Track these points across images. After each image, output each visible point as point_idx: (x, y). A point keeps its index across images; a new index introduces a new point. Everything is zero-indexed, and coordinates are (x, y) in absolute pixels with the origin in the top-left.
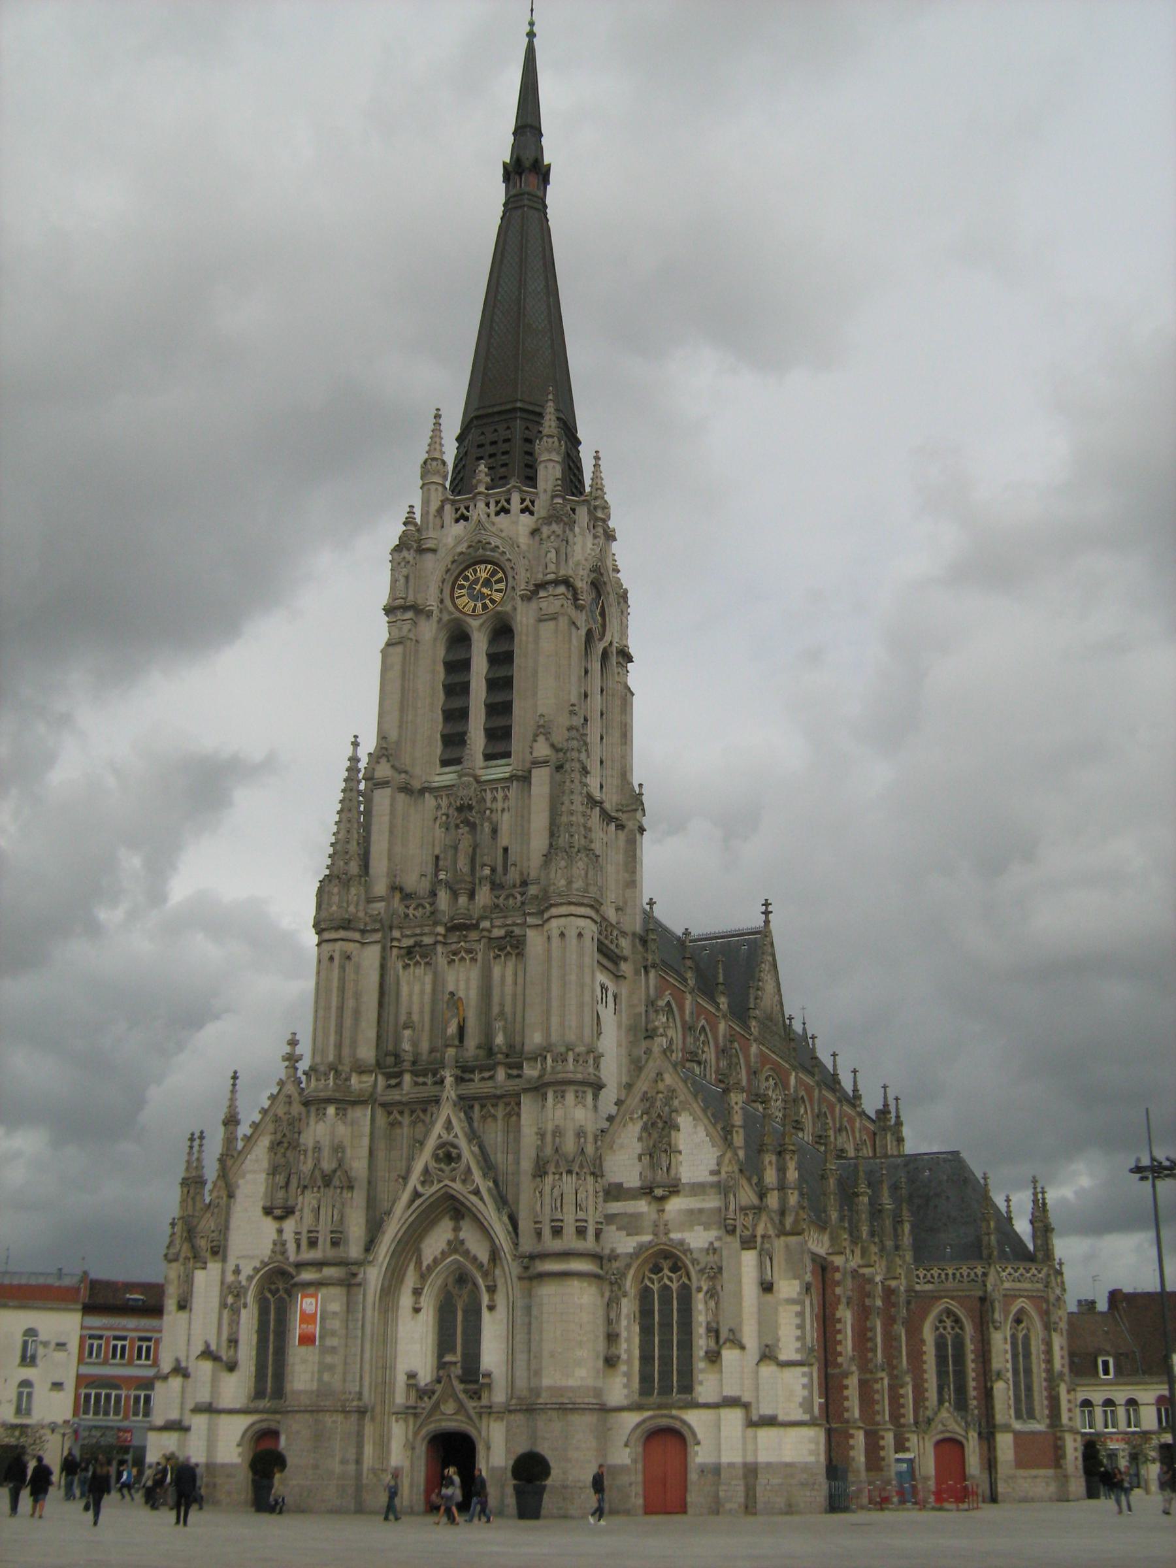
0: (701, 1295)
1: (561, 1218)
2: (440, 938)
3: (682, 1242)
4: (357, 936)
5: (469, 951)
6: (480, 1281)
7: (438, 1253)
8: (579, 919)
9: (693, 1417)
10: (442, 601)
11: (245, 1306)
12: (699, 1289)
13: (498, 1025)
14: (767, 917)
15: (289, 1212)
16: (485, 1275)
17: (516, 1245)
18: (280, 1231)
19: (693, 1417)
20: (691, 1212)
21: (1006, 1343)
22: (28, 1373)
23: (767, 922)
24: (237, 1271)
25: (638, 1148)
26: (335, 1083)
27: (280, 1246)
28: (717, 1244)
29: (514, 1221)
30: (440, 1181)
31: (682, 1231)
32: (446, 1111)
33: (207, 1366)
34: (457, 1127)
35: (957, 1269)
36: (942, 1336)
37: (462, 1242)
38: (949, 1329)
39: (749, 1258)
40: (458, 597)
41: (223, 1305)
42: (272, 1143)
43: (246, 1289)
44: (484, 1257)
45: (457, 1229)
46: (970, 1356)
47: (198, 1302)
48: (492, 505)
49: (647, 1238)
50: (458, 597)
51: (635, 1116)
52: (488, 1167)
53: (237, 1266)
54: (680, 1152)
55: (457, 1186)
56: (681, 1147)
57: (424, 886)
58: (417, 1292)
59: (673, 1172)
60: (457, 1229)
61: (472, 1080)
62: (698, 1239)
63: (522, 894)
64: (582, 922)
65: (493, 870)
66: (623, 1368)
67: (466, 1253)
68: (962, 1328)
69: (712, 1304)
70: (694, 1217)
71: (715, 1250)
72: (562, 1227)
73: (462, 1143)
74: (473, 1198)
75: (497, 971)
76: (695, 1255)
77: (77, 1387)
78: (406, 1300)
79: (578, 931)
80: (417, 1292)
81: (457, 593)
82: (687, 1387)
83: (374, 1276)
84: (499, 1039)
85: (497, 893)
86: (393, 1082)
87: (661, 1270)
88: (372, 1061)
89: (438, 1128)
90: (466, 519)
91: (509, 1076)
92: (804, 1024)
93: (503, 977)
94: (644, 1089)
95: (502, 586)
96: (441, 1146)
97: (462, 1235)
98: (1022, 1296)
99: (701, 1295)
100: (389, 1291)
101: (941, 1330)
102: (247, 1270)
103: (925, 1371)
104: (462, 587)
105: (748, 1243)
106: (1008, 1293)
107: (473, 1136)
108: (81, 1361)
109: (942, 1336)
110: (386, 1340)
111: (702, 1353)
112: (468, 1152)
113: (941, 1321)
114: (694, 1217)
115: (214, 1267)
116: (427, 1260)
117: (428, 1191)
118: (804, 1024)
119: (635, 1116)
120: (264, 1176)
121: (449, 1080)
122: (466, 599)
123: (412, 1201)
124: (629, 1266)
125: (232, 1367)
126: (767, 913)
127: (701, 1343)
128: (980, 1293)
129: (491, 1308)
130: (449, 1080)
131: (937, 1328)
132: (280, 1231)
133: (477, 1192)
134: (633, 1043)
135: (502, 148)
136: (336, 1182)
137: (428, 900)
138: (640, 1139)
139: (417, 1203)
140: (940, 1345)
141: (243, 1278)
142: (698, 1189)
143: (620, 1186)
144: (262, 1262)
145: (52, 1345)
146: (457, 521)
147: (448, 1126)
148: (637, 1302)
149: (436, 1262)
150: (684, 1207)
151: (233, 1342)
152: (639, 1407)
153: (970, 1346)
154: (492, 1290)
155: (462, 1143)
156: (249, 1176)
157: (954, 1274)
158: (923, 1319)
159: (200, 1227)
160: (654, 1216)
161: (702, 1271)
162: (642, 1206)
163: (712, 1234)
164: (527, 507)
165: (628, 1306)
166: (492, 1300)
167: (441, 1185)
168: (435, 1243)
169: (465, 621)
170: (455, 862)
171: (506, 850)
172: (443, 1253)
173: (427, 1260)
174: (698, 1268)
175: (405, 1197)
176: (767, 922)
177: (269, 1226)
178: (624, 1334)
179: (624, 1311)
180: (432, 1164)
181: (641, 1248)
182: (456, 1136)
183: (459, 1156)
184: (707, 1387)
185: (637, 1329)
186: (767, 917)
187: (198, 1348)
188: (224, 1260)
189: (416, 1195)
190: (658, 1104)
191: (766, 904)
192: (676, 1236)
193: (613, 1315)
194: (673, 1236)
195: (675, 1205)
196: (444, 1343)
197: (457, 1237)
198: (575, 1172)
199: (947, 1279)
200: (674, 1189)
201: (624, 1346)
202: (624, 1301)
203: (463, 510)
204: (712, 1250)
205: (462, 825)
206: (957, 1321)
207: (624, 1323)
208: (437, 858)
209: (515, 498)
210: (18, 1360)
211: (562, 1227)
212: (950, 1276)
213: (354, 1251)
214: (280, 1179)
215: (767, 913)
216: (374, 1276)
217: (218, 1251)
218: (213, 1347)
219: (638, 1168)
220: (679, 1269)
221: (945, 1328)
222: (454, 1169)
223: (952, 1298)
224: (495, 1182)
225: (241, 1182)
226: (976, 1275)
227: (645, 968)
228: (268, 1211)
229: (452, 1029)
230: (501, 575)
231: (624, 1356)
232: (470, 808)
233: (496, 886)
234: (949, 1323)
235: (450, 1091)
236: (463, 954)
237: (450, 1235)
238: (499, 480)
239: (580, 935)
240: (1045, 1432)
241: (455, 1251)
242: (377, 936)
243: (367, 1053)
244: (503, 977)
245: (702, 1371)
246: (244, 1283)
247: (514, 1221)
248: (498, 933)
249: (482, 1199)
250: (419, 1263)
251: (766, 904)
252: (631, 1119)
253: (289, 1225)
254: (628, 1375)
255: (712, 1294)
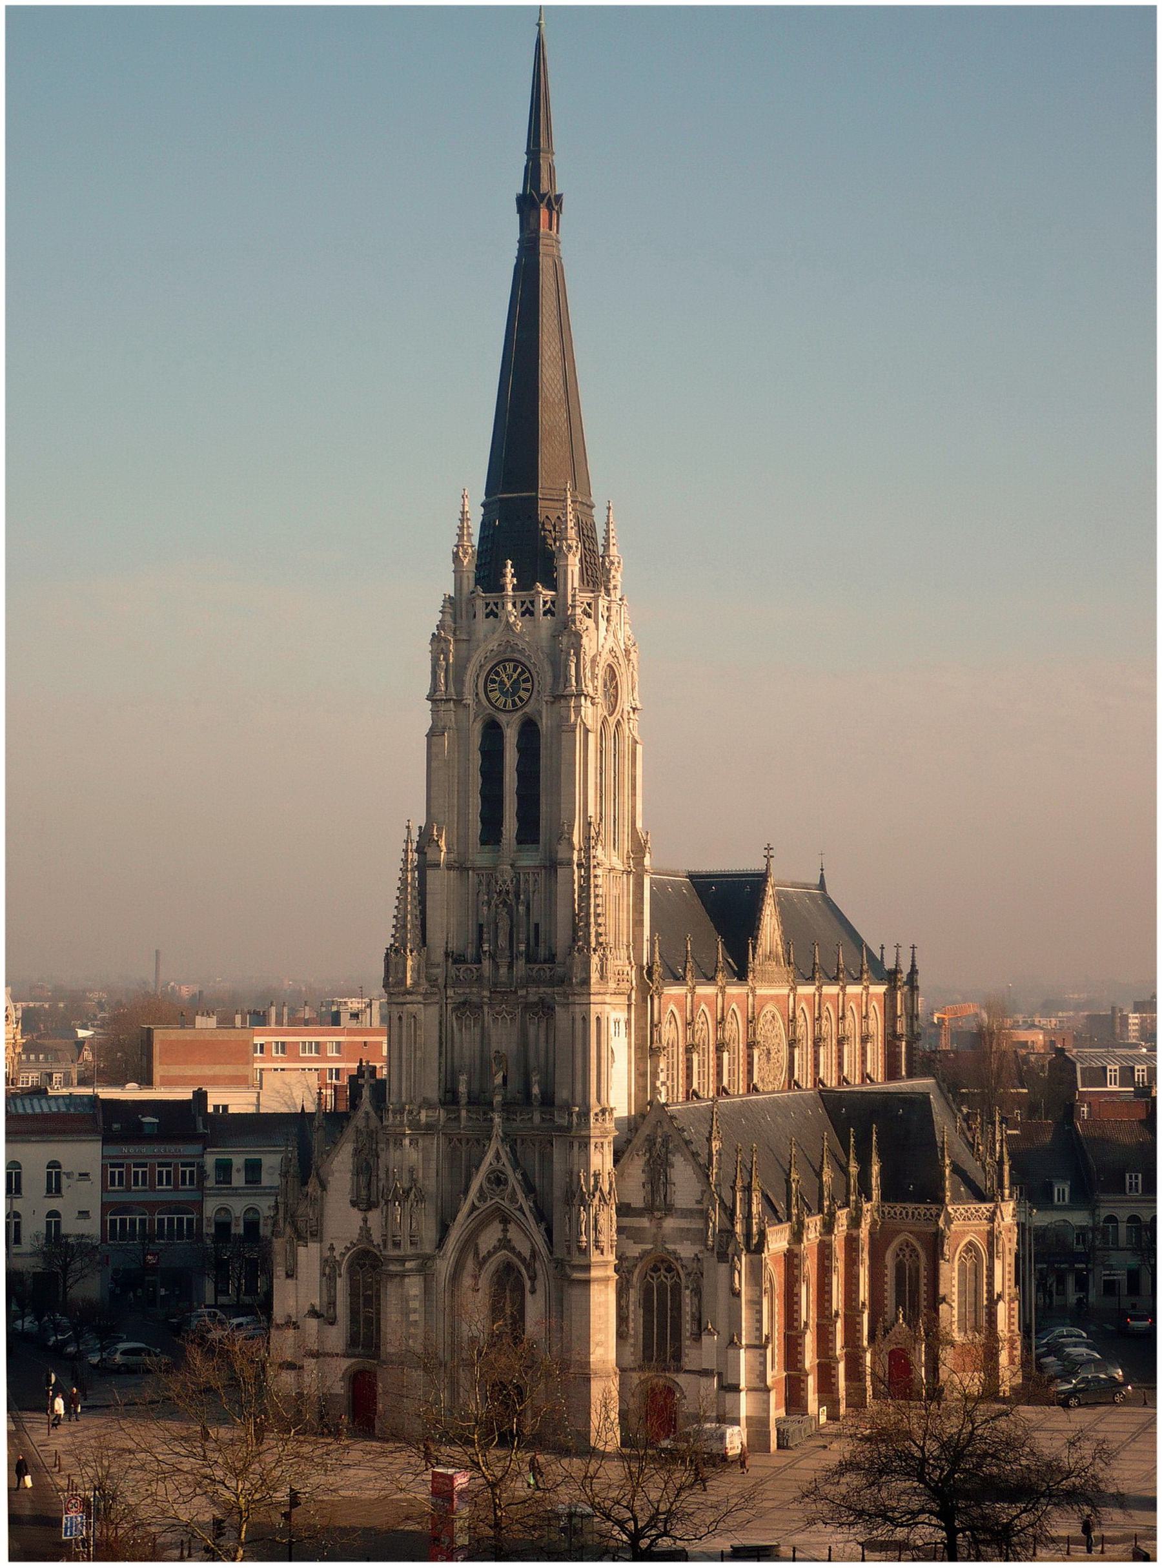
0: (688, 1292)
2: (485, 1000)
3: (674, 1252)
4: (420, 998)
5: (509, 1013)
6: (524, 1271)
7: (491, 1248)
9: (682, 1379)
10: (477, 694)
11: (340, 1276)
12: (687, 1288)
13: (535, 1078)
15: (370, 1206)
16: (527, 1267)
17: (551, 1253)
18: (365, 1220)
19: (682, 1379)
20: (682, 1230)
22: (55, 1204)
24: (332, 1248)
25: (642, 1178)
26: (408, 1120)
27: (366, 1231)
28: (700, 1256)
29: (549, 1232)
30: (492, 1199)
31: (674, 1243)
32: (494, 1146)
33: (313, 1323)
34: (504, 1159)
35: (916, 1209)
36: (901, 1262)
37: (509, 1241)
38: (907, 1257)
39: (723, 1268)
40: (491, 691)
41: (323, 1274)
42: (355, 1150)
43: (340, 1265)
44: (527, 1254)
45: (505, 1230)
46: (923, 1281)
47: (302, 1272)
48: (518, 605)
49: (649, 1247)
50: (491, 691)
51: (640, 1153)
52: (529, 1189)
53: (332, 1244)
54: (674, 1184)
55: (506, 1203)
56: (675, 1181)
57: (470, 952)
58: (476, 1277)
59: (668, 1199)
60: (505, 1230)
61: (514, 1120)
62: (686, 1250)
63: (551, 969)
65: (528, 945)
66: (632, 1341)
67: (512, 1249)
68: (917, 1256)
69: (696, 1300)
70: (683, 1234)
71: (699, 1259)
73: (509, 1171)
74: (518, 1213)
75: (532, 1030)
76: (684, 1262)
77: (103, 1215)
78: (467, 1281)
80: (476, 1277)
81: (490, 686)
82: (677, 1356)
83: (443, 1267)
84: (536, 1090)
85: (531, 966)
86: (452, 1116)
87: (660, 1270)
88: (436, 1100)
89: (489, 1157)
90: (496, 616)
91: (543, 1120)
92: (822, 870)
93: (537, 1036)
94: (647, 1132)
95: (528, 685)
96: (493, 1172)
97: (509, 1235)
99: (688, 1292)
100: (455, 1277)
102: (340, 1248)
104: (493, 681)
105: (723, 1257)
107: (516, 1164)
108: (104, 1189)
109: (901, 1262)
110: (455, 1313)
111: (688, 1334)
112: (513, 1179)
113: (901, 1249)
114: (683, 1234)
115: (314, 1247)
116: (483, 1253)
117: (483, 1206)
118: (822, 870)
119: (640, 1153)
120: (350, 1175)
121: (497, 1120)
122: (497, 694)
123: (471, 1213)
124: (636, 1266)
125: (332, 1322)
126: (768, 858)
127: (688, 1327)
128: (933, 1230)
129: (533, 1292)
130: (497, 1120)
131: (898, 1255)
132: (365, 1220)
133: (521, 1209)
135: (517, 186)
136: (412, 1196)
137: (476, 966)
138: (643, 1171)
139: (476, 1213)
140: (900, 1268)
141: (336, 1254)
142: (687, 1213)
143: (628, 1205)
144: (351, 1243)
145: (76, 1176)
146: (487, 616)
147: (498, 1157)
148: (642, 1293)
149: (490, 1254)
150: (676, 1226)
151: (332, 1304)
152: (641, 1368)
153: (923, 1273)
154: (533, 1278)
155: (509, 1171)
156: (336, 1174)
157: (913, 1213)
159: (299, 1212)
160: (654, 1230)
161: (689, 1274)
162: (645, 1222)
163: (696, 1249)
164: (549, 608)
165: (634, 1295)
166: (533, 1286)
167: (493, 1201)
168: (489, 1239)
170: (496, 937)
171: (537, 926)
172: (494, 1247)
173: (483, 1253)
174: (687, 1272)
175: (465, 1208)
177: (356, 1216)
178: (632, 1316)
179: (632, 1299)
180: (486, 1185)
181: (645, 1253)
182: (504, 1165)
183: (506, 1179)
184: (692, 1358)
185: (641, 1312)
187: (307, 1308)
188: (321, 1241)
189: (474, 1208)
190: (658, 1146)
192: (670, 1247)
193: (623, 1303)
194: (667, 1246)
195: (670, 1223)
196: (496, 1311)
197: (505, 1236)
199: (907, 1216)
200: (669, 1210)
201: (631, 1325)
203: (492, 606)
204: (697, 1259)
205: (501, 906)
206: (914, 1250)
207: (632, 1308)
208: (481, 926)
210: (44, 1193)
212: (910, 1214)
213: (428, 1249)
214: (363, 1180)
215: (768, 858)
216: (443, 1267)
217: (317, 1234)
218: (318, 1308)
219: (642, 1193)
220: (673, 1270)
221: (904, 1256)
222: (503, 1190)
223: (910, 1233)
224: (535, 1202)
225: (330, 1178)
226: (931, 1215)
228: (354, 1204)
229: (498, 1080)
230: (527, 675)
231: (632, 1332)
232: (508, 892)
233: (530, 959)
234: (907, 1250)
235: (498, 1130)
236: (504, 1014)
237: (500, 1235)
238: (524, 584)
241: (505, 1248)
242: (436, 999)
243: (433, 1094)
244: (537, 1036)
245: (688, 1347)
246: (338, 1258)
247: (549, 1232)
248: (533, 998)
249: (524, 1214)
250: (477, 1254)
251: (769, 848)
252: (638, 1155)
253: (374, 1216)
254: (634, 1346)
255: (697, 1292)
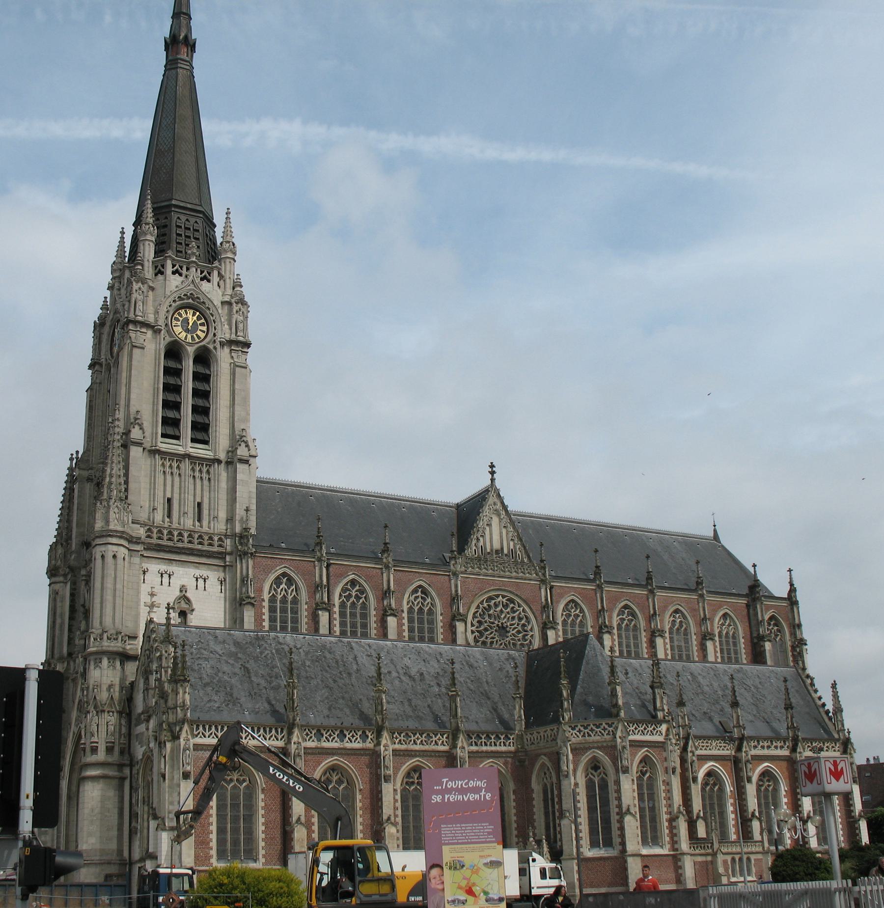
1: (97, 740)
8: (114, 546)
14: (493, 476)
21: (633, 783)
23: (493, 480)
35: (545, 732)
64: (115, 548)
72: (97, 747)
79: (113, 554)
98: (594, 748)
101: (545, 780)
103: (534, 814)
106: (578, 746)
126: (493, 473)
134: (235, 610)
157: (544, 736)
158: (532, 773)
169: (184, 347)
176: (493, 480)
186: (493, 476)
191: (492, 466)
198: (107, 711)
202: (140, 789)
209: (169, 263)
211: (97, 747)
215: (493, 473)
227: (240, 556)
239: (114, 557)
240: (616, 857)
251: (492, 466)
